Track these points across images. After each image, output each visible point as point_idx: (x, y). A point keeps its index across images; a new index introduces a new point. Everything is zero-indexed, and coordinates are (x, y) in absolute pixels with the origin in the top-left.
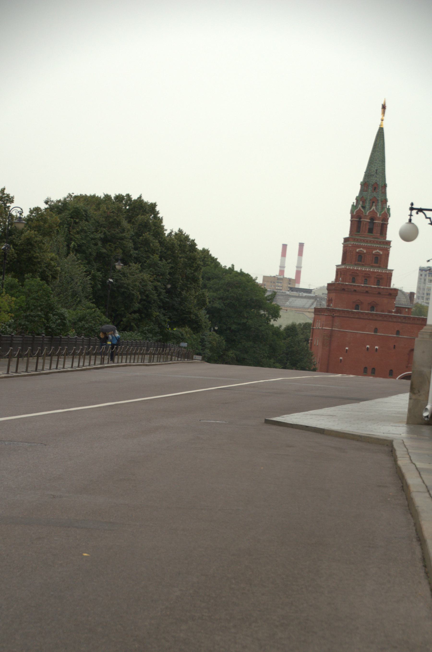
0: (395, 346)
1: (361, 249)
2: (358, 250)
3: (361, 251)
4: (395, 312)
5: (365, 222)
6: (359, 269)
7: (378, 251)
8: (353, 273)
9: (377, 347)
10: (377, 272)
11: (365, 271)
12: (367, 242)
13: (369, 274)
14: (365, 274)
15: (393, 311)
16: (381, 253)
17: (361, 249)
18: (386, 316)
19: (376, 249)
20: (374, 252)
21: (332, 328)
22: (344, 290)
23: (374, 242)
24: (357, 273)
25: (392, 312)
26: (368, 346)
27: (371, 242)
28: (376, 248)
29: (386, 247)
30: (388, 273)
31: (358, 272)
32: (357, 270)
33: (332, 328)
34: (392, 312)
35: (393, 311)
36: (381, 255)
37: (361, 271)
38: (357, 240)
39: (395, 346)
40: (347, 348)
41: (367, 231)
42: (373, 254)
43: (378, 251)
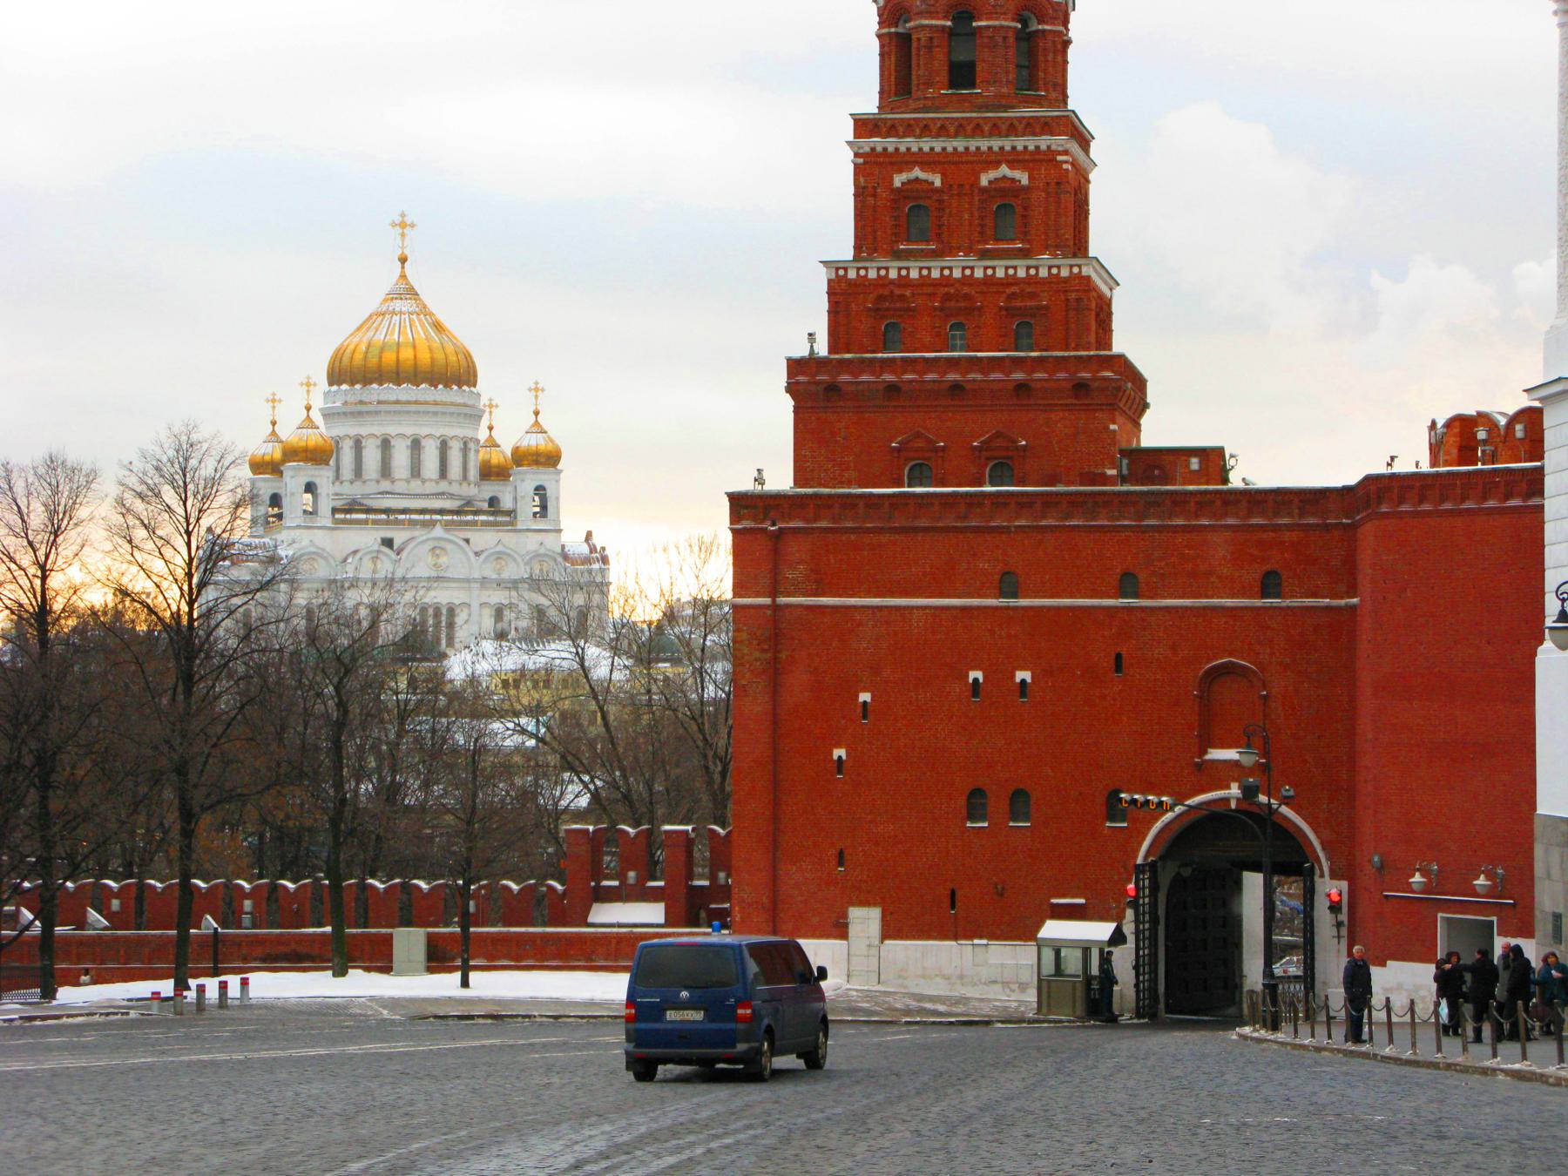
0: (1118, 657)
1: (917, 173)
2: (898, 180)
3: (917, 179)
4: (1124, 480)
5: (924, 36)
6: (914, 274)
7: (1004, 170)
8: (881, 298)
9: (1023, 675)
10: (1011, 281)
11: (946, 281)
12: (942, 131)
13: (967, 297)
14: (947, 297)
15: (1112, 472)
16: (1023, 178)
17: (917, 173)
18: (1074, 503)
19: (996, 164)
20: (984, 181)
21: (774, 594)
22: (832, 389)
23: (977, 130)
24: (902, 298)
25: (1105, 480)
26: (976, 674)
27: (961, 129)
28: (992, 159)
29: (1044, 142)
30: (1066, 280)
31: (908, 293)
32: (903, 282)
33: (774, 594)
34: (1105, 480)
35: (1112, 472)
36: (1025, 189)
37: (924, 281)
38: (892, 129)
39: (1118, 657)
40: (865, 697)
41: (943, 76)
42: (983, 190)
43: (1004, 170)
